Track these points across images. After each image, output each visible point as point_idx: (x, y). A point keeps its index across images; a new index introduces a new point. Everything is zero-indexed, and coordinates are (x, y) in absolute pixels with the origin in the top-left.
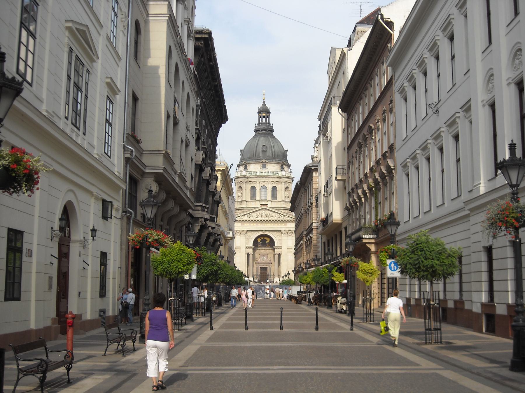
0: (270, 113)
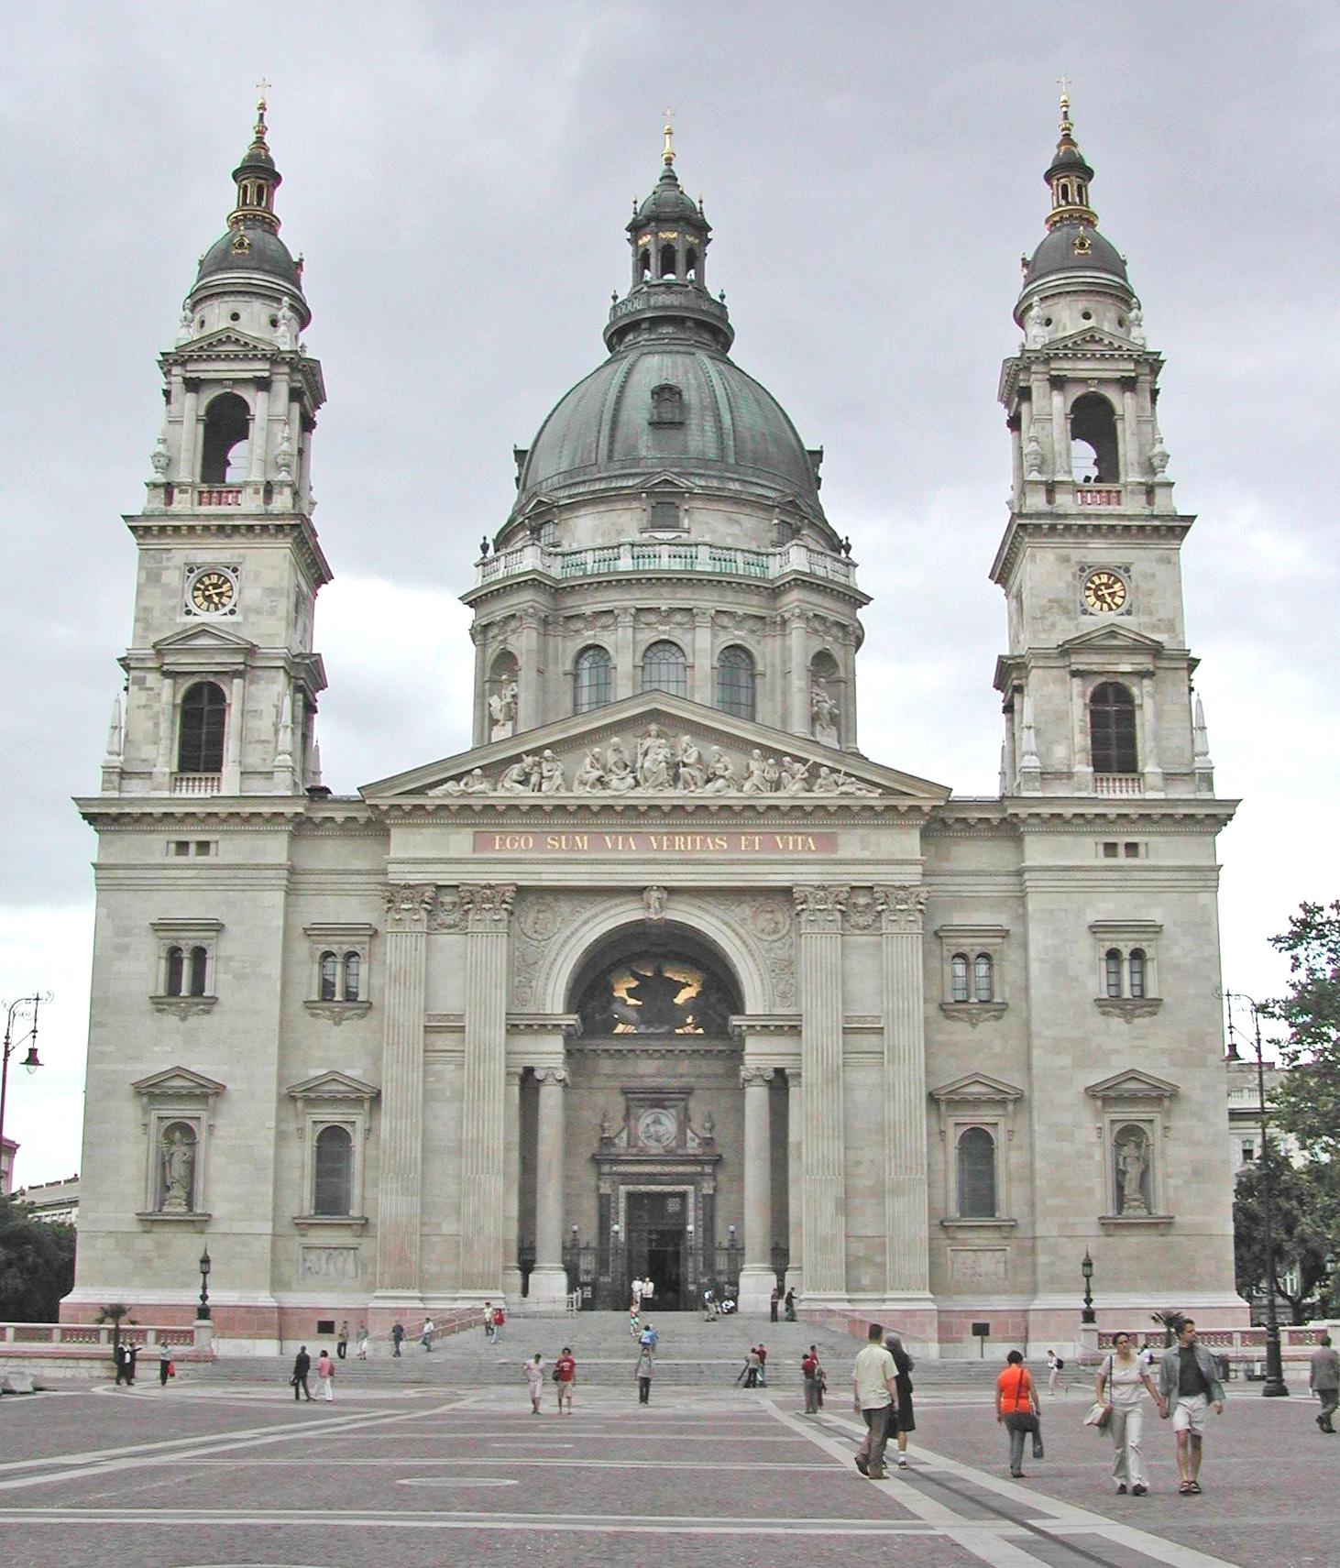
0: (701, 229)
